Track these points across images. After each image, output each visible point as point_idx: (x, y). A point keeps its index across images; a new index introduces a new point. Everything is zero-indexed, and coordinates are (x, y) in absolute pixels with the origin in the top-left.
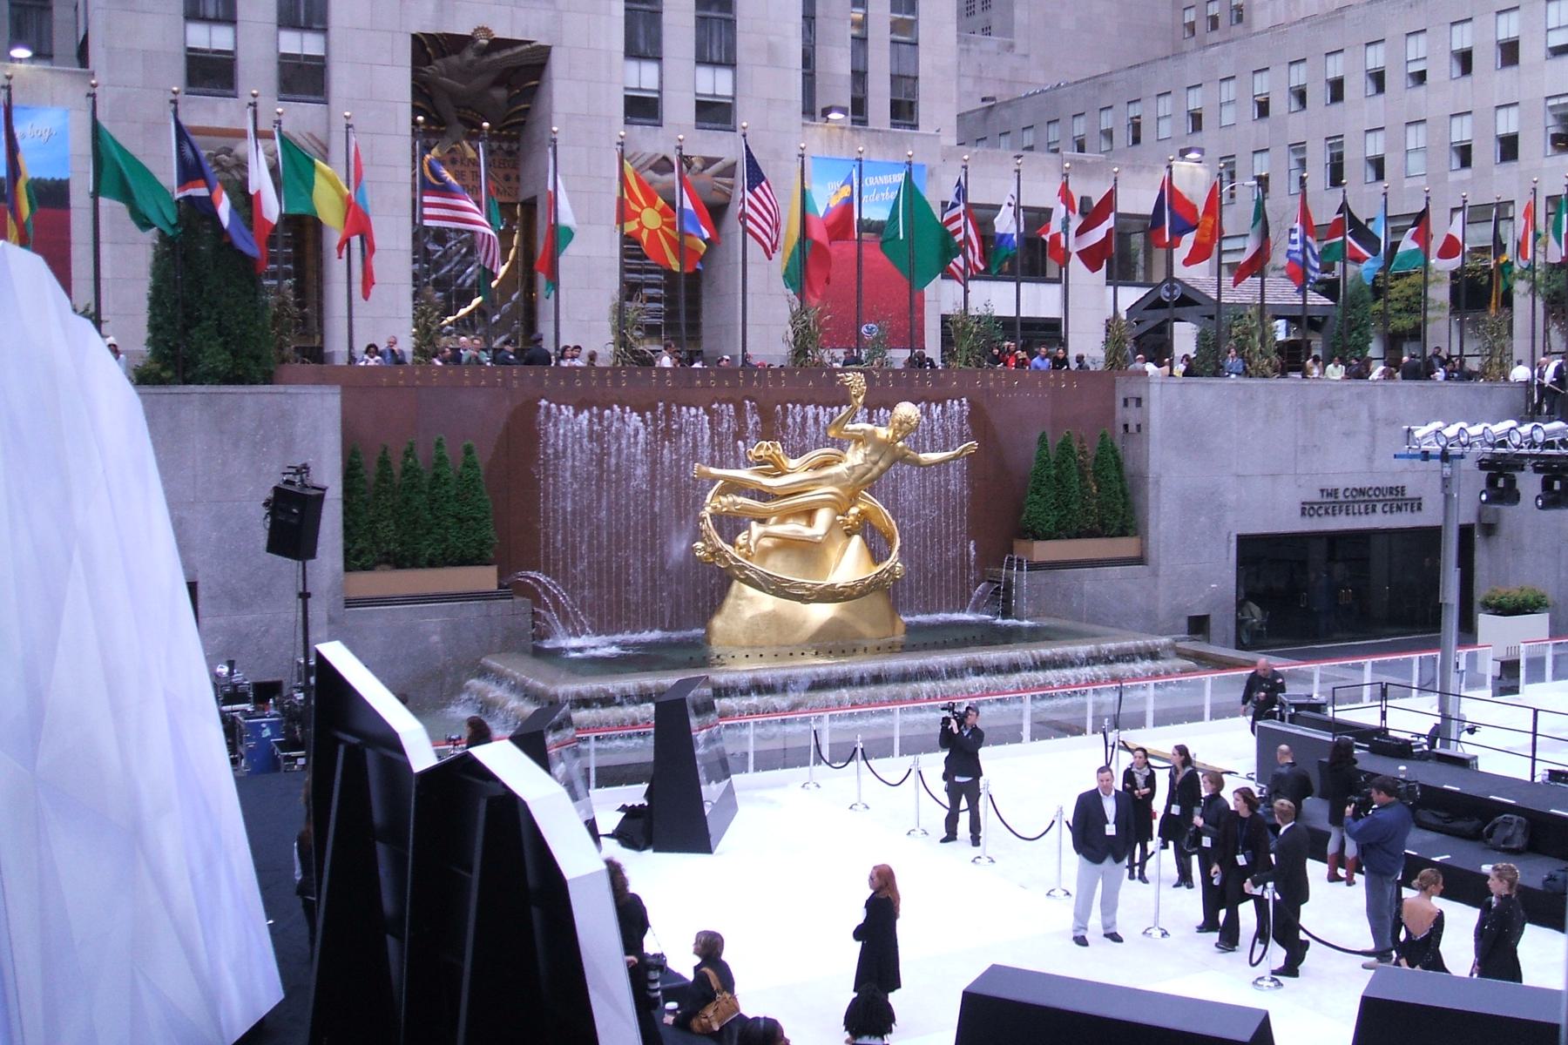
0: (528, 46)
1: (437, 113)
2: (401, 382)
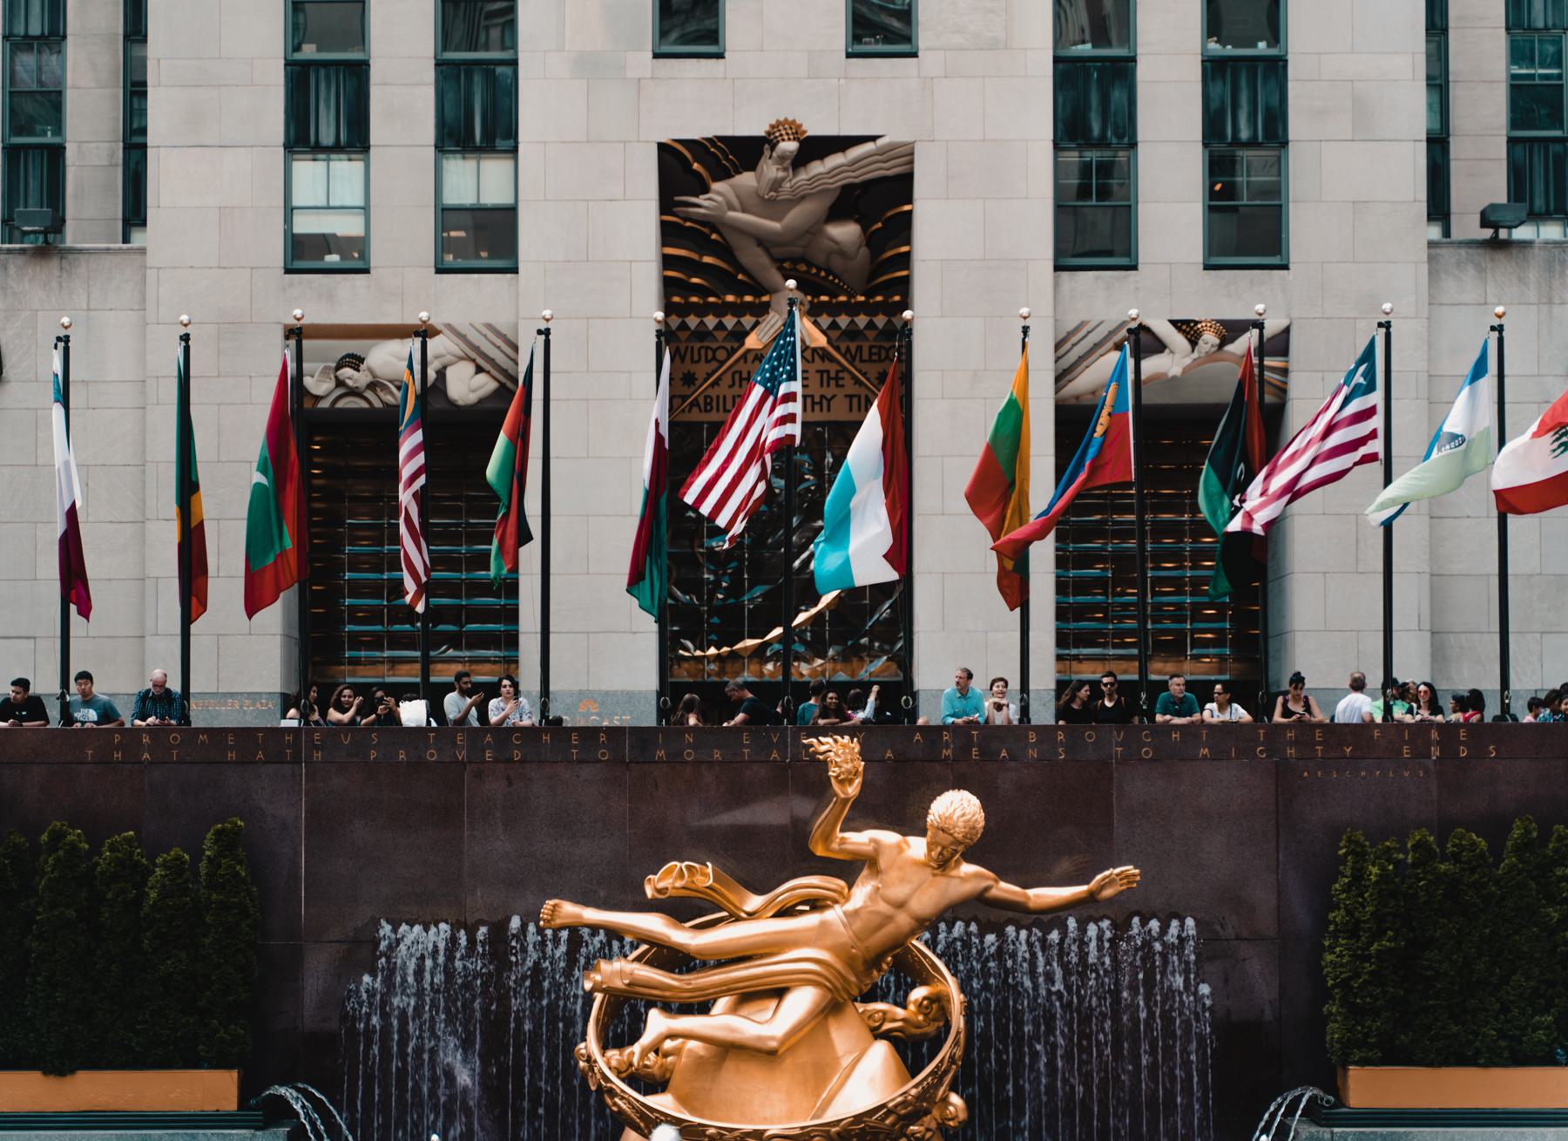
0: (869, 147)
1: (745, 272)
2: (118, 755)
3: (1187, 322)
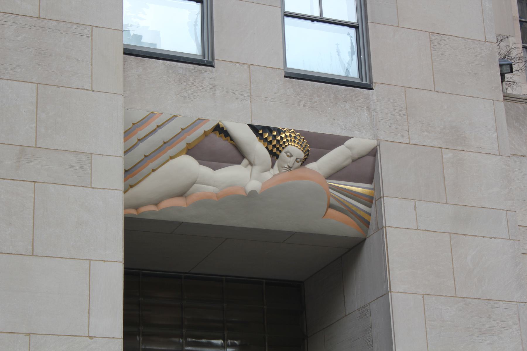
3: (270, 130)
